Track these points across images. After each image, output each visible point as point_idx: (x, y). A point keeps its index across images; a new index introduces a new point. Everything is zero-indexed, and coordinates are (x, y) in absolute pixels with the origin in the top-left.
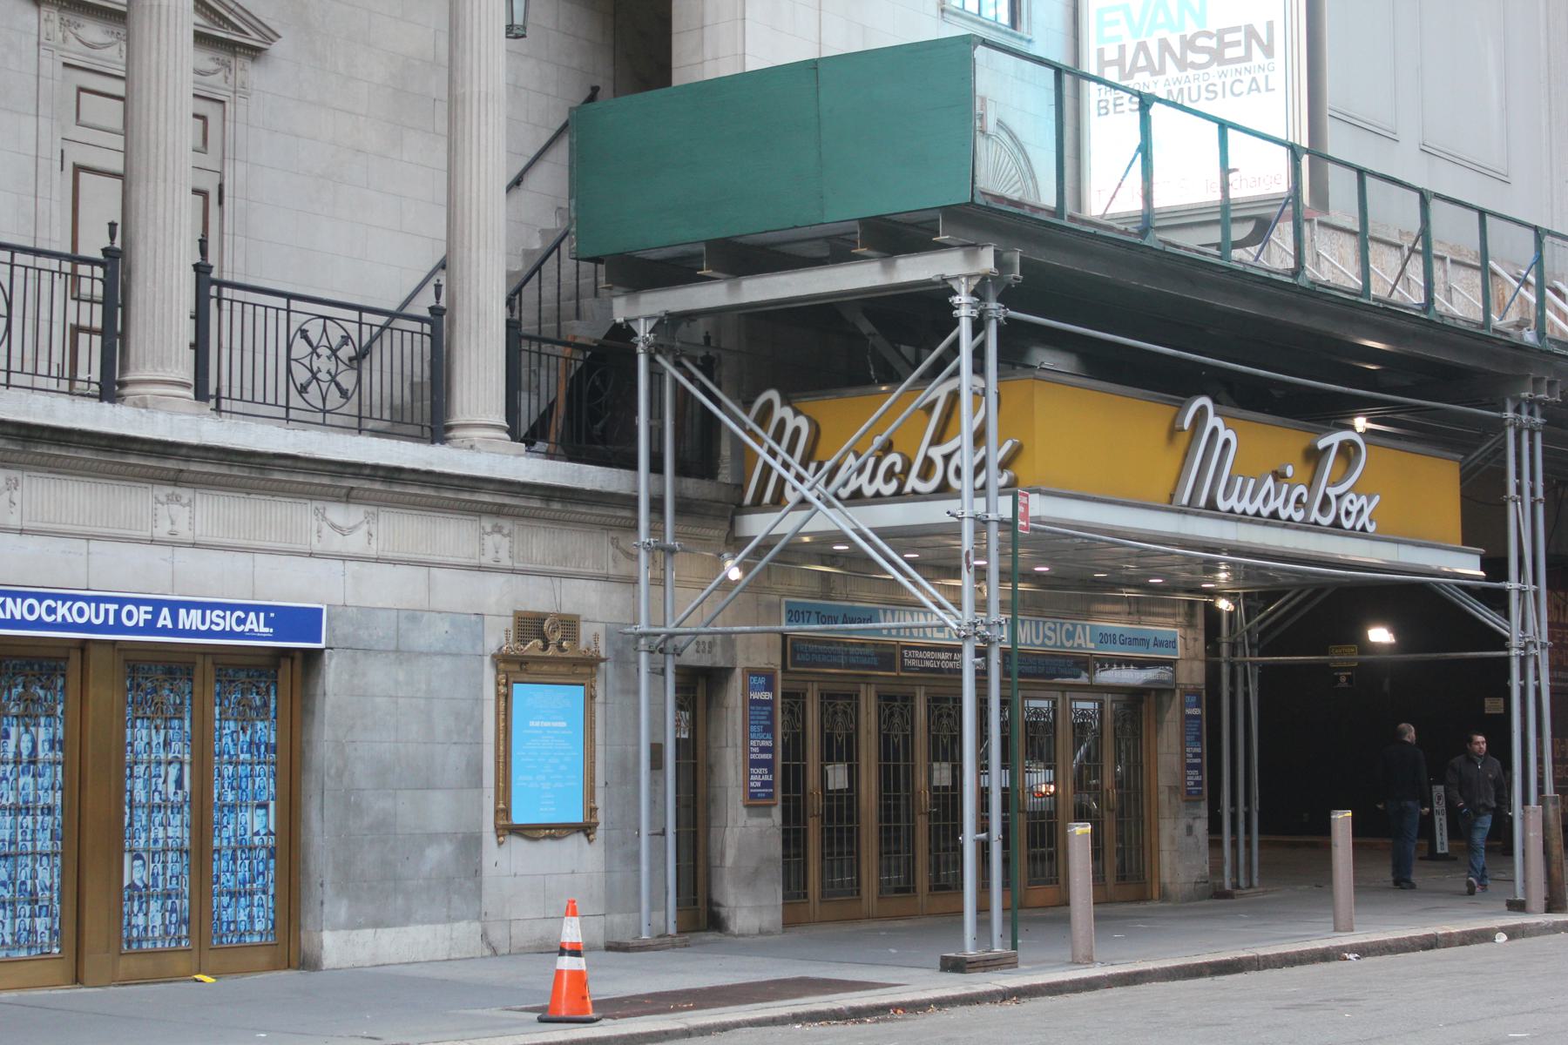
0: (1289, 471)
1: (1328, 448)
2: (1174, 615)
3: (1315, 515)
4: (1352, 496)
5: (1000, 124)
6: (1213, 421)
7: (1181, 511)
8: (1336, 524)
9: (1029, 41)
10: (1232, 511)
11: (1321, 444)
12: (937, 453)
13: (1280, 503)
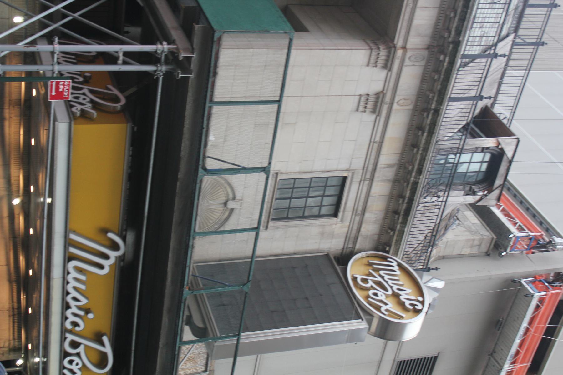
0: (90, 316)
1: (103, 345)
2: (14, 339)
3: (70, 337)
4: (80, 365)
5: (232, 210)
6: (113, 254)
7: (66, 236)
8: (66, 354)
9: (267, 227)
10: (68, 283)
11: (105, 339)
12: (85, 91)
13: (74, 310)
